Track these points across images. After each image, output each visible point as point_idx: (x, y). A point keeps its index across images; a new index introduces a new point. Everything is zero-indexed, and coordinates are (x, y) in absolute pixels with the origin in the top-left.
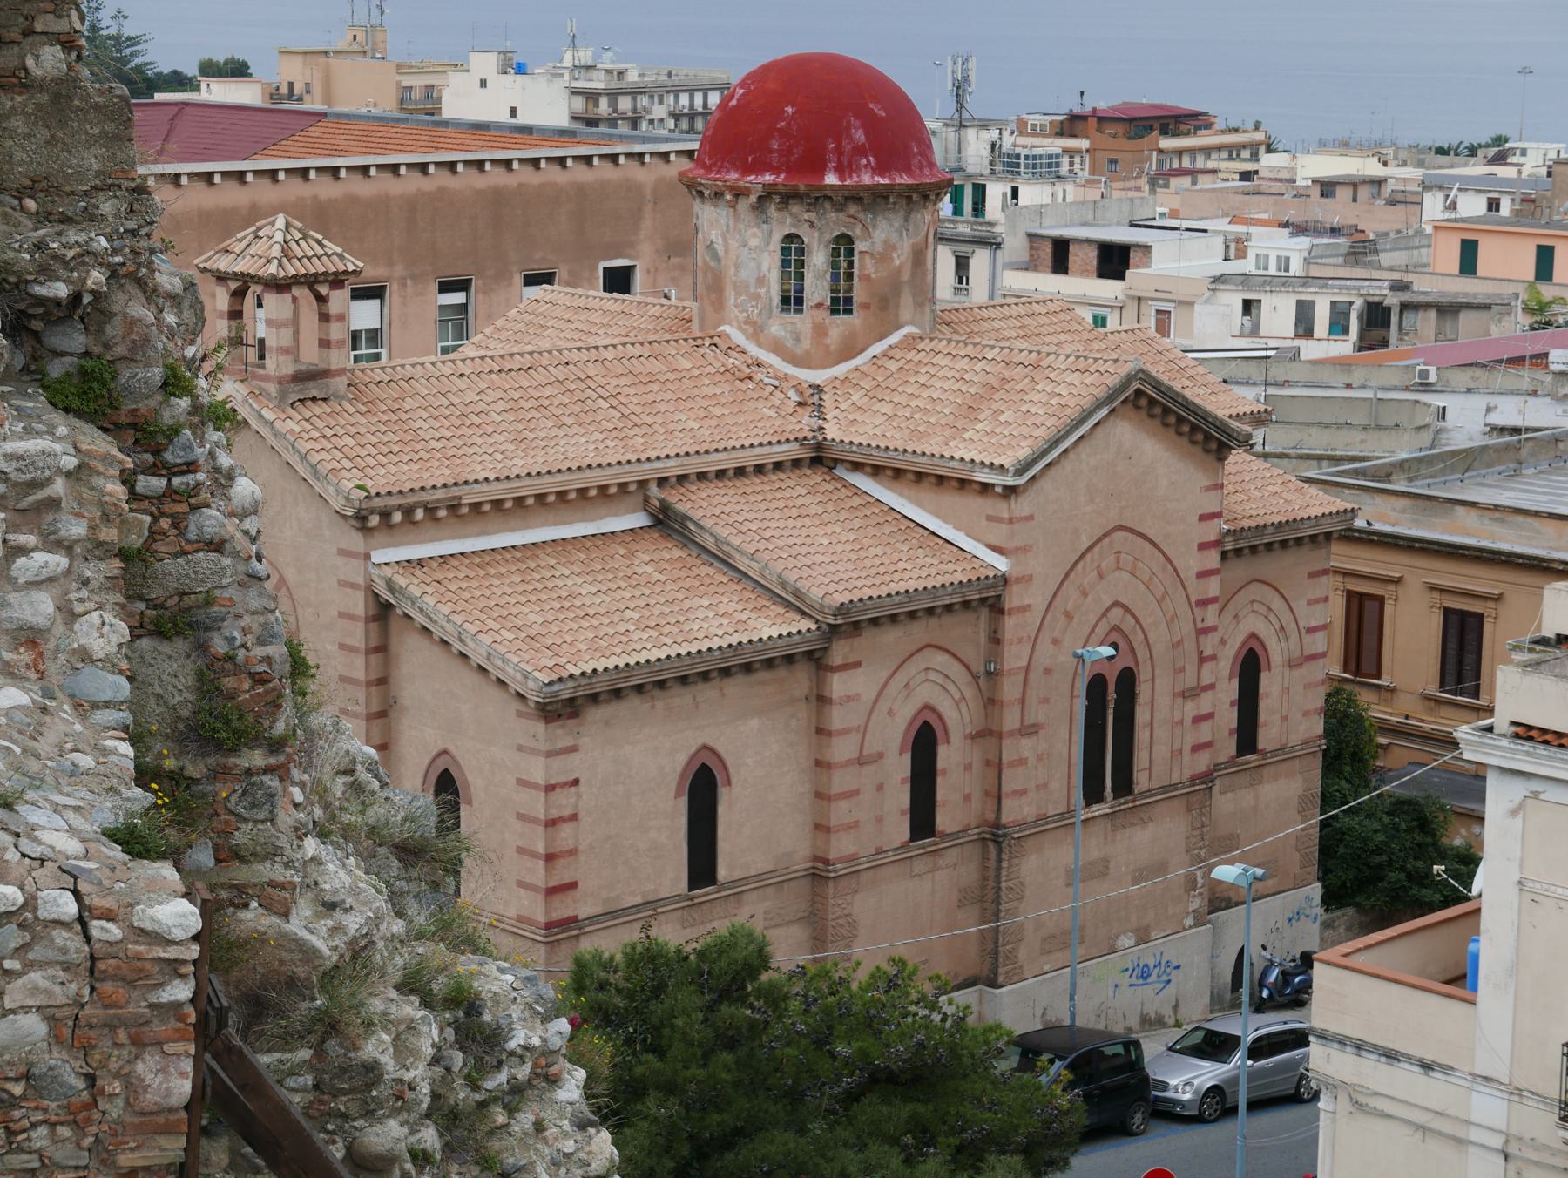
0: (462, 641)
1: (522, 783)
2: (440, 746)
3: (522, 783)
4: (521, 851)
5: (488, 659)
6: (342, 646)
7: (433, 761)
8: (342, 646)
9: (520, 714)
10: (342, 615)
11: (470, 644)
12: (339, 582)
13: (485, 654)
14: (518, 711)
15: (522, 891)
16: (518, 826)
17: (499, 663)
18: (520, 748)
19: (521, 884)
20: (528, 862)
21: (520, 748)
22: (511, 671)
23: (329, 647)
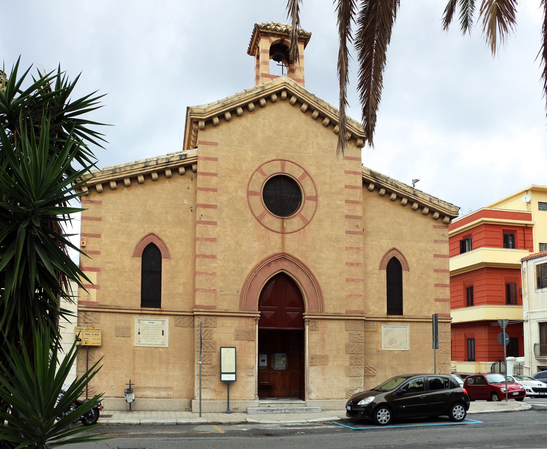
0: (415, 195)
1: (436, 256)
2: (391, 247)
3: (436, 256)
4: (436, 285)
5: (431, 202)
6: (347, 201)
7: (386, 254)
8: (347, 201)
9: (435, 227)
10: (347, 187)
11: (421, 196)
12: (346, 172)
13: (428, 199)
14: (434, 226)
15: (438, 303)
16: (435, 275)
17: (436, 202)
18: (436, 241)
19: (437, 300)
20: (441, 290)
21: (436, 241)
22: (443, 205)
23: (338, 203)
